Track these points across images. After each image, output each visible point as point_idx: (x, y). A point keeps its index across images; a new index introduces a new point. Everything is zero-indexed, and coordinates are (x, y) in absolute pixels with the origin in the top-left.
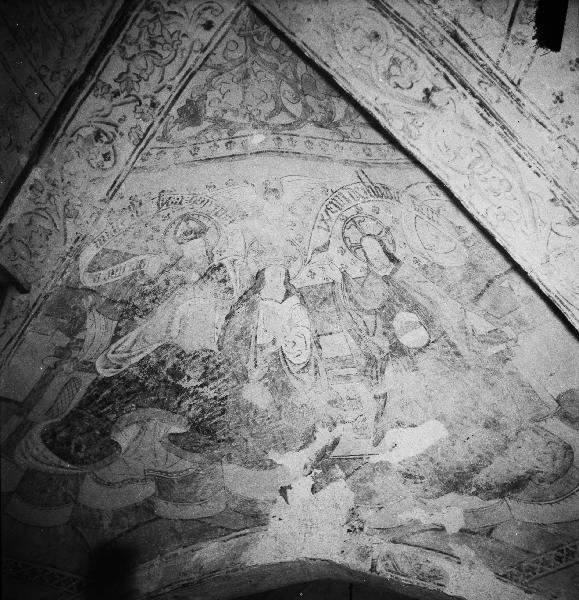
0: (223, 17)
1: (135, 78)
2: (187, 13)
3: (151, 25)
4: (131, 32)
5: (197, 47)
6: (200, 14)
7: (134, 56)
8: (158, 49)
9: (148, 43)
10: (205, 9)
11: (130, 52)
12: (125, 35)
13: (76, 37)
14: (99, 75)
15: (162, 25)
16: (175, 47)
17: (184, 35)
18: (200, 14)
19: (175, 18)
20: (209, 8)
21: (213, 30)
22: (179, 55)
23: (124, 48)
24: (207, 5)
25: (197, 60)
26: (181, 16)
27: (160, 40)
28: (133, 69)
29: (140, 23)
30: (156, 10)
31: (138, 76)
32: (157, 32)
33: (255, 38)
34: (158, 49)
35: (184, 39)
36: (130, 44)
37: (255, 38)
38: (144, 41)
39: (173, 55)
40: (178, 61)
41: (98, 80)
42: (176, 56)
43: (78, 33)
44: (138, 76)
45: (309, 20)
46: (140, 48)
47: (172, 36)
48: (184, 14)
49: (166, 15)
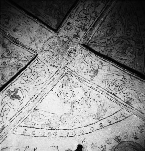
0: (65, 26)
1: (93, 5)
2: (75, 28)
3: (86, 23)
4: (93, 21)
5: (72, 17)
6: (71, 27)
7: (92, 13)
8: (84, 16)
9: (87, 18)
10: (69, 29)
11: (93, 15)
12: (95, 20)
13: (115, 14)
14: (105, 6)
15: (83, 24)
16: (79, 16)
17: (76, 20)
18: (71, 27)
19: (78, 26)
20: (68, 29)
21: (67, 22)
22: (78, 14)
23: (96, 16)
24: (69, 30)
25: (73, 12)
26: (77, 27)
27: (84, 19)
28: (93, 8)
29: (89, 24)
30: (84, 29)
31: (92, 6)
32: (84, 21)
33: (59, 13)
34: (84, 16)
35: (76, 19)
36: (93, 17)
37: (59, 13)
38: (89, 18)
39: (80, 13)
40: (79, 11)
41: (106, 4)
42: (79, 13)
43: (114, 15)
44: (92, 6)
45: (36, 31)
46: (90, 16)
47: (80, 20)
48: (76, 28)
49: (81, 27)
